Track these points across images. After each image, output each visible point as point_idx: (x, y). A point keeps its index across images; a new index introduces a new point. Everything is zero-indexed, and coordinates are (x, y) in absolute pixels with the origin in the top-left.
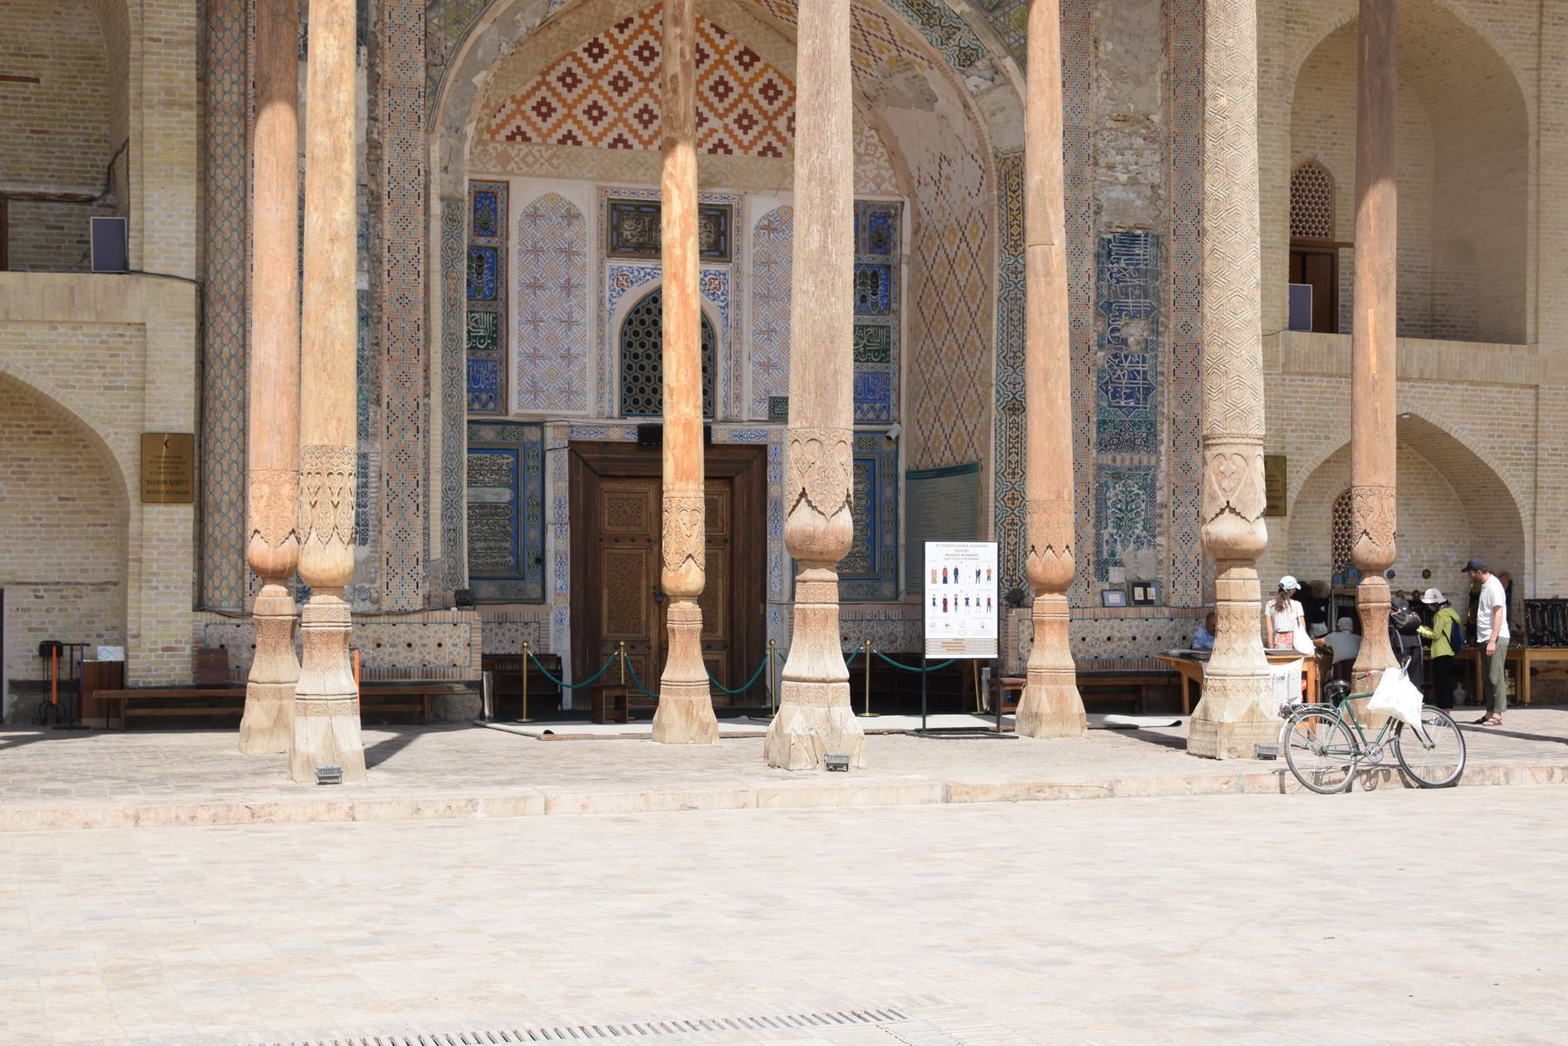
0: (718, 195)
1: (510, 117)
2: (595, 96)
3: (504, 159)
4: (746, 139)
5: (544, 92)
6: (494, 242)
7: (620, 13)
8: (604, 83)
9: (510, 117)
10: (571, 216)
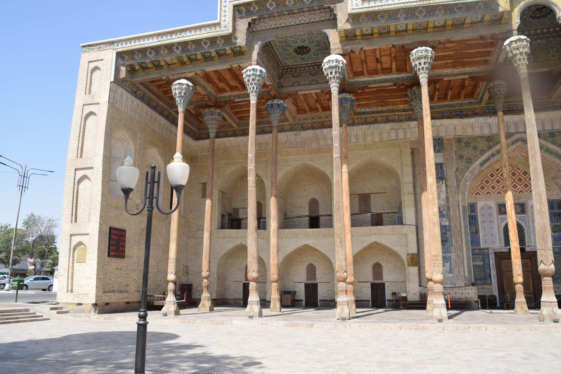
0: (521, 201)
1: (476, 190)
2: (493, 184)
3: (475, 198)
4: (527, 189)
5: (482, 185)
6: (475, 214)
7: (496, 168)
8: (494, 182)
9: (476, 190)
10: (490, 208)
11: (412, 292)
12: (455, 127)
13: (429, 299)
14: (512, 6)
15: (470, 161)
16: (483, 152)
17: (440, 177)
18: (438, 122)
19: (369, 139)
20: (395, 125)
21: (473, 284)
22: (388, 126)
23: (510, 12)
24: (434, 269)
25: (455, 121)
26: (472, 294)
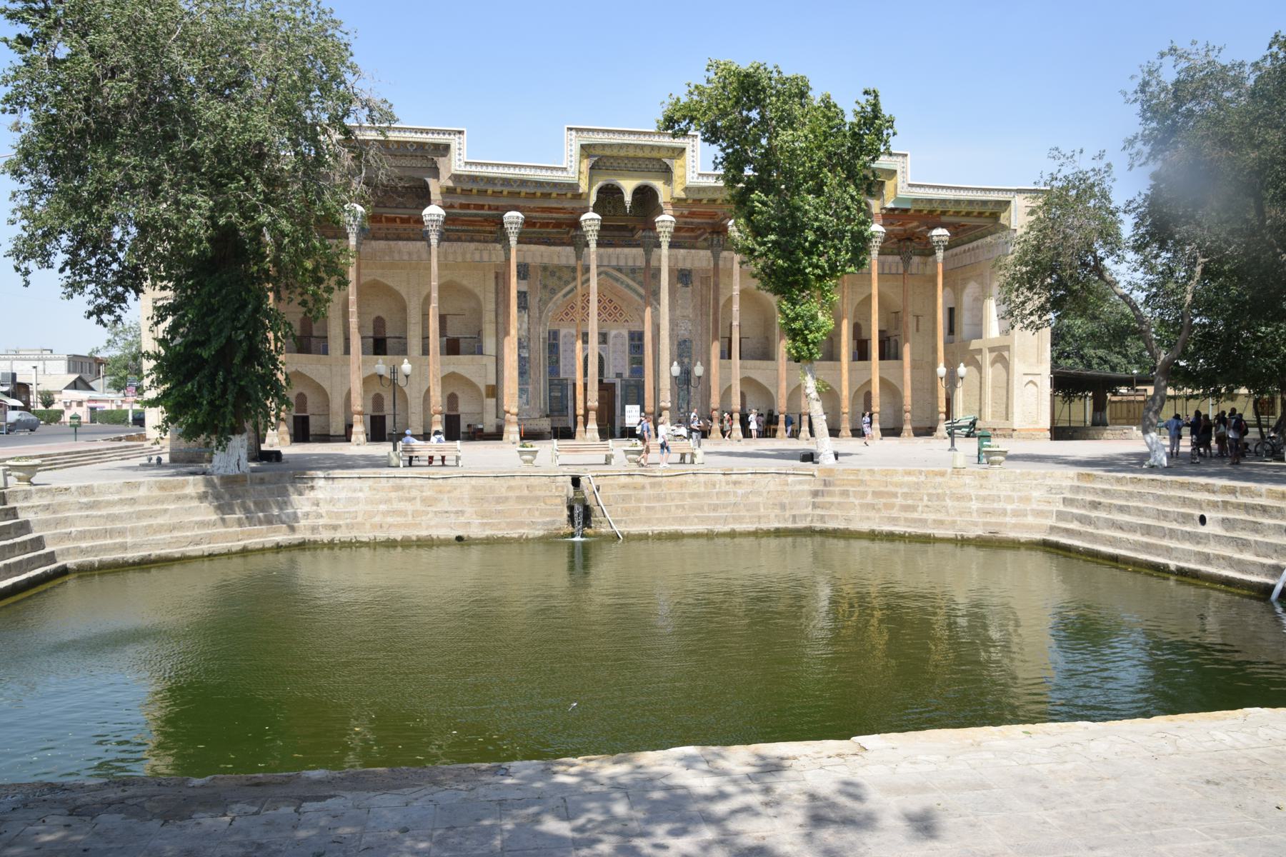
11: (489, 424)
12: (541, 254)
15: (553, 292)
16: (567, 283)
17: (523, 306)
19: (451, 258)
20: (481, 246)
21: (547, 416)
22: (473, 245)
24: (511, 401)
25: (543, 248)
26: (545, 425)
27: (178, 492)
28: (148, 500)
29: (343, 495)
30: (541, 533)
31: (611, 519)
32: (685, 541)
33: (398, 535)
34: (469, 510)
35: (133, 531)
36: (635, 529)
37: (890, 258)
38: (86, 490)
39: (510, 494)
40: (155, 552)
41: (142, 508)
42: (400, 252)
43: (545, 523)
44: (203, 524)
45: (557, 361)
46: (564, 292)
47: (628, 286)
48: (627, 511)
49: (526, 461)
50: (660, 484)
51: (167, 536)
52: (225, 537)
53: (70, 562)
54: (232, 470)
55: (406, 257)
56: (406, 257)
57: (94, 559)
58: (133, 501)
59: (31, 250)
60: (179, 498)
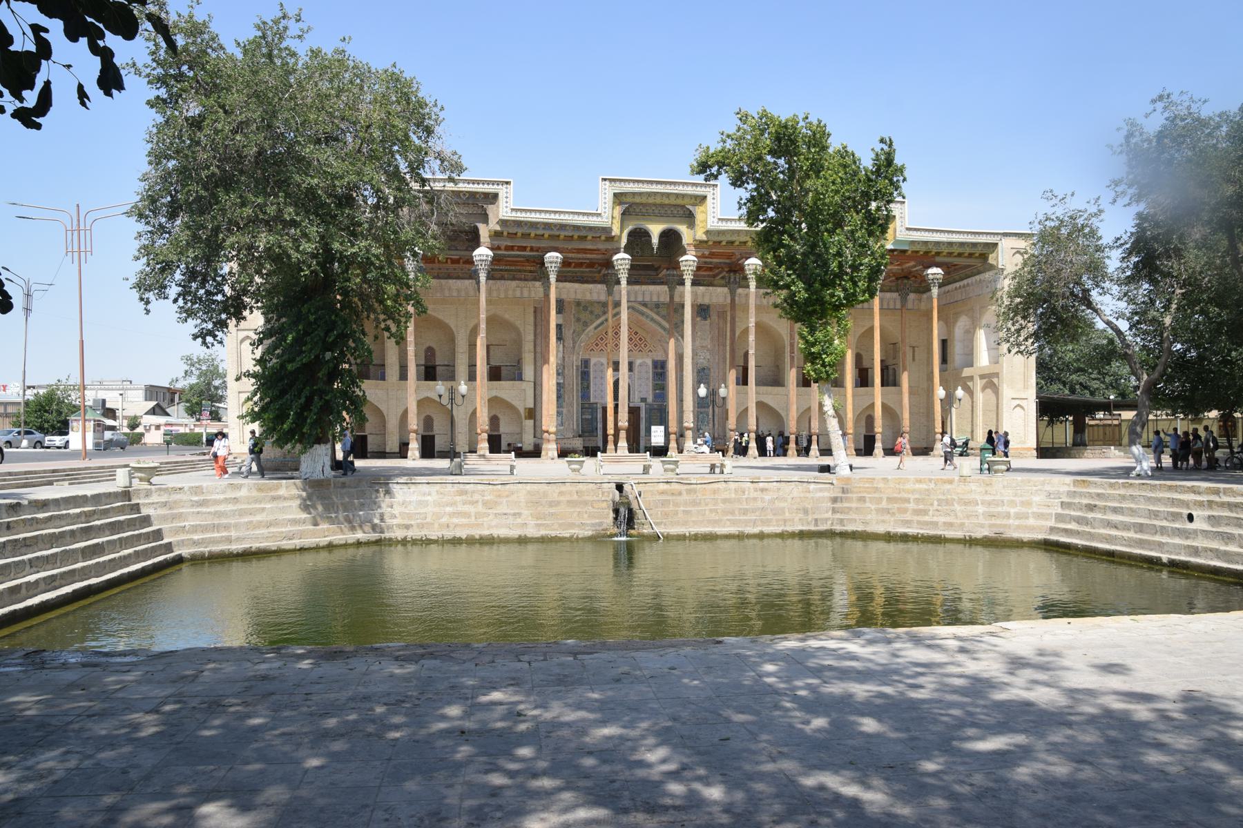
11: (528, 443)
12: (576, 291)
13: (544, 446)
14: (622, 231)
15: (586, 324)
16: (598, 317)
17: (560, 338)
18: (561, 285)
20: (522, 283)
22: (514, 283)
23: (620, 237)
24: (549, 421)
25: (577, 285)
27: (272, 494)
28: (248, 500)
29: (414, 498)
30: (590, 533)
31: (653, 521)
32: (719, 542)
33: (463, 534)
34: (525, 512)
35: (236, 526)
36: (674, 530)
37: (888, 295)
38: (197, 490)
39: (562, 498)
40: (256, 545)
41: (244, 506)
42: (450, 289)
43: (593, 525)
44: (295, 522)
45: (588, 387)
46: (595, 324)
47: (652, 319)
48: (666, 515)
49: (574, 470)
50: (695, 491)
51: (264, 531)
52: (314, 534)
53: (185, 552)
54: (318, 475)
55: (455, 294)
56: (455, 294)
57: (206, 550)
58: (236, 500)
59: (151, 285)
60: (274, 499)
